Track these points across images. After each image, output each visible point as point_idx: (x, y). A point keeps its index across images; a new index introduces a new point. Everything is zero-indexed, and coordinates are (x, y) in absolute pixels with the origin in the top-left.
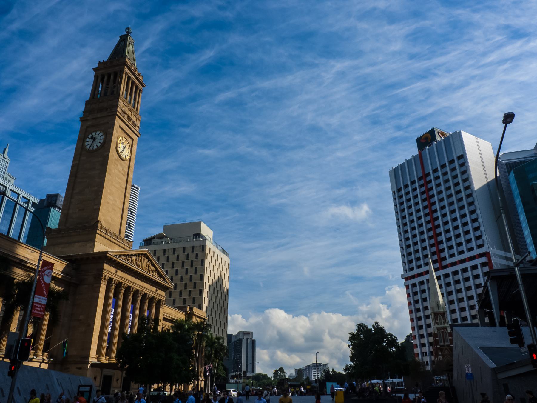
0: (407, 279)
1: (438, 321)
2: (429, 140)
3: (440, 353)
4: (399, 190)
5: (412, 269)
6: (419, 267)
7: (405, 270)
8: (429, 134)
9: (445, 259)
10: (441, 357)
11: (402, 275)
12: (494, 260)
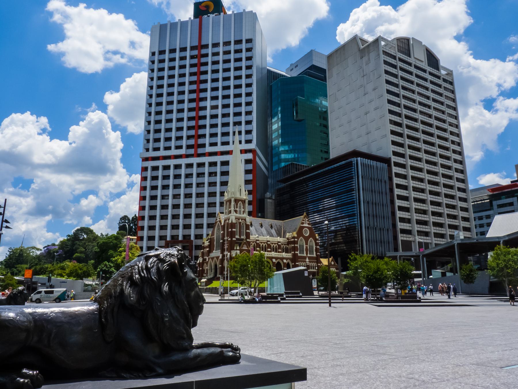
1: (238, 209)
2: (211, 11)
3: (238, 248)
4: (162, 52)
5: (157, 149)
6: (169, 148)
7: (147, 150)
9: (204, 146)
10: (238, 252)
11: (141, 153)
12: (258, 160)
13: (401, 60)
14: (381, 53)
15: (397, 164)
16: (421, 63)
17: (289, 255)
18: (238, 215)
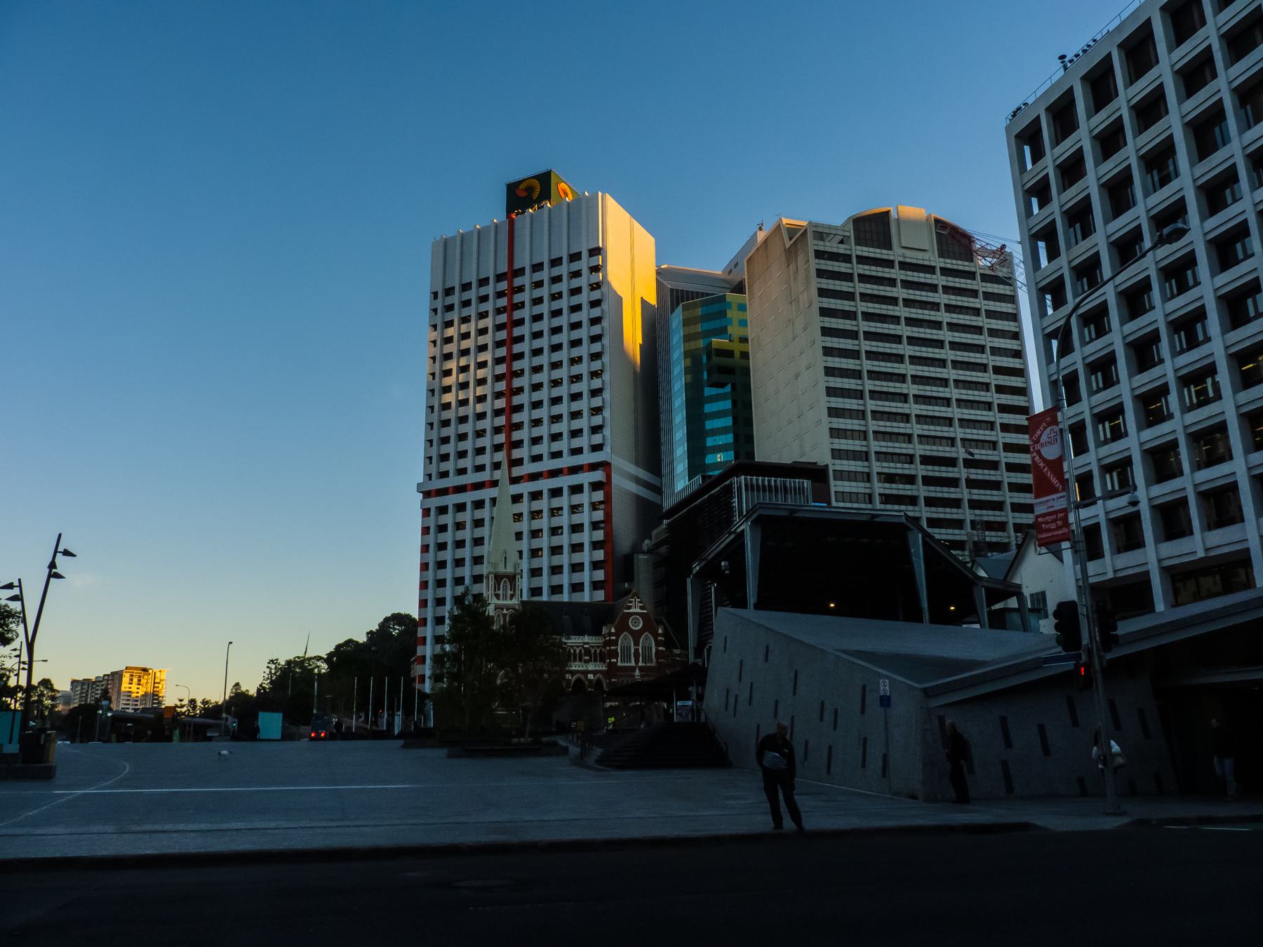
0: (427, 494)
1: (501, 592)
2: (535, 196)
4: (449, 292)
5: (444, 475)
8: (536, 183)
12: (616, 479)
13: (862, 260)
14: (812, 255)
15: (840, 475)
16: (920, 255)
17: (602, 667)
18: (501, 602)
